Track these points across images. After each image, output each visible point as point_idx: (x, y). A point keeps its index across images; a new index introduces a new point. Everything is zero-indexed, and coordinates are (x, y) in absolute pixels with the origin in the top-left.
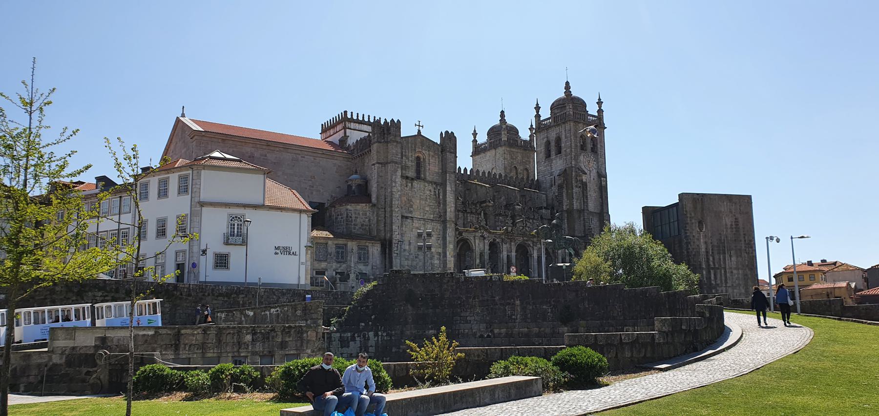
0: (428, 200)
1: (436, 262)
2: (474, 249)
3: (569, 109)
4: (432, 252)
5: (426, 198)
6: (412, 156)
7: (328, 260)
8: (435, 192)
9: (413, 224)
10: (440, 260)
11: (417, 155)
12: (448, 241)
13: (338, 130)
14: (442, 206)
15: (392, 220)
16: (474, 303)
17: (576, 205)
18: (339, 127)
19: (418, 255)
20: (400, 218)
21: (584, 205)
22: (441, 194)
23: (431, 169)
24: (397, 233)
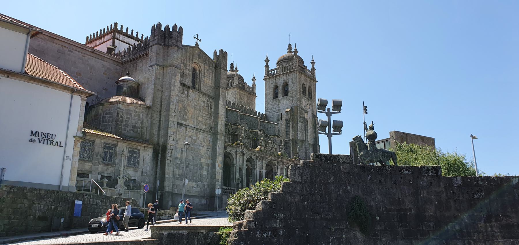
0: (202, 111)
1: (205, 173)
2: (235, 163)
3: (295, 62)
4: (202, 163)
5: (200, 108)
6: (189, 65)
7: (93, 161)
8: (208, 104)
9: (186, 132)
10: (208, 171)
11: (194, 66)
12: (218, 152)
13: (105, 40)
14: (213, 118)
15: (168, 124)
16: (489, 229)
17: (300, 137)
18: (106, 38)
19: (189, 164)
20: (176, 123)
21: (305, 137)
22: (213, 107)
23: (205, 82)
24: (172, 139)
